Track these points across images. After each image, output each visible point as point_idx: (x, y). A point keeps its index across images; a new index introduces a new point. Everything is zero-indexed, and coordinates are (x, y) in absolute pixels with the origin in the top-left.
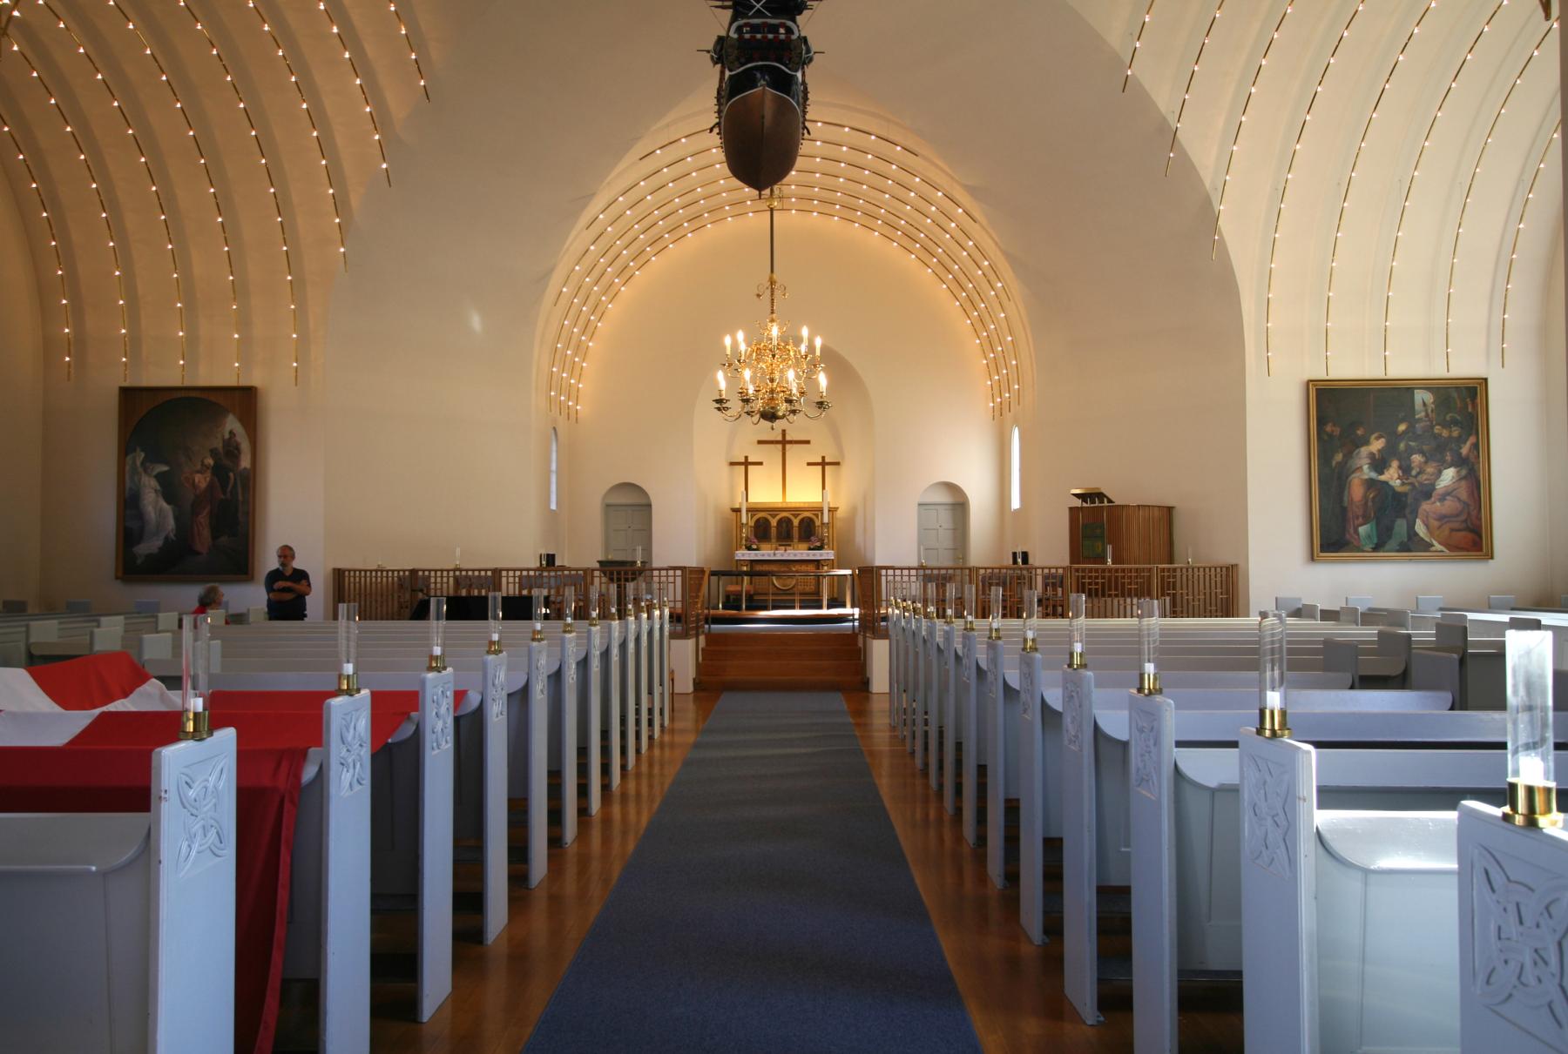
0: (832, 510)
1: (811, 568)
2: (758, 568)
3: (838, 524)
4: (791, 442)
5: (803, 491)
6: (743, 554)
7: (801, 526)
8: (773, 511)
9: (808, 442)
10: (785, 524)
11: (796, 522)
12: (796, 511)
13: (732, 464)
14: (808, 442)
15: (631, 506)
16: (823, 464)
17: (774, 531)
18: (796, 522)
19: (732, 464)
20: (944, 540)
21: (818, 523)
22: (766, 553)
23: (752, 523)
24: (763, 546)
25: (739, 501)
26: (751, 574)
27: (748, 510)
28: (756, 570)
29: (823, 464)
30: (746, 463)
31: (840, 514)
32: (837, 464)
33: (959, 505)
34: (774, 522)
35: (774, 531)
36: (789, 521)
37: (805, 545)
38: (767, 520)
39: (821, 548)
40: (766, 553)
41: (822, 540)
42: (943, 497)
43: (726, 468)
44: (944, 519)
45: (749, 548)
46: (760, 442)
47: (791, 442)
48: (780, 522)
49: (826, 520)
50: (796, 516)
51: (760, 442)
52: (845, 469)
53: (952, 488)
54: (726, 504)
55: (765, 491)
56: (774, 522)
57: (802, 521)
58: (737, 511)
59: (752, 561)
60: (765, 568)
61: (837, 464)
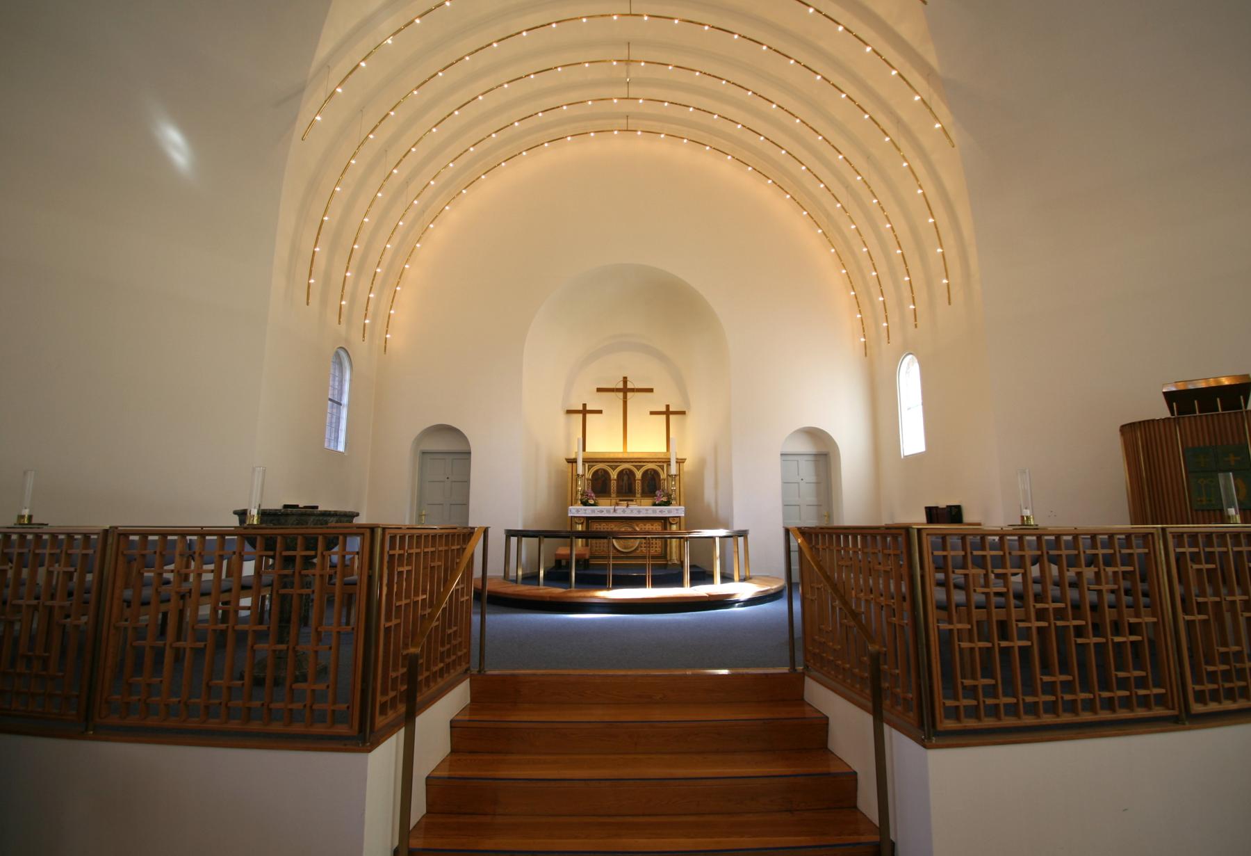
0: (680, 462)
1: (657, 527)
2: (596, 527)
3: (685, 479)
4: (633, 390)
5: (645, 441)
6: (578, 510)
7: (646, 480)
8: (614, 462)
9: (651, 390)
10: (627, 476)
11: (639, 475)
12: (639, 462)
13: (569, 412)
14: (651, 390)
15: (447, 453)
16: (668, 413)
17: (614, 485)
18: (639, 475)
19: (569, 412)
20: (807, 494)
21: (663, 476)
22: (604, 509)
23: (589, 475)
24: (601, 501)
25: (576, 451)
26: (585, 535)
27: (584, 461)
28: (593, 530)
29: (668, 413)
30: (584, 412)
31: (687, 466)
32: (683, 413)
33: (823, 454)
34: (614, 475)
35: (614, 485)
36: (630, 474)
37: (649, 501)
38: (606, 472)
39: (668, 503)
40: (604, 509)
41: (669, 496)
42: (804, 447)
43: (562, 417)
44: (806, 471)
45: (585, 503)
46: (599, 390)
47: (633, 390)
48: (621, 474)
49: (673, 471)
50: (639, 468)
51: (599, 390)
52: (690, 419)
53: (815, 435)
54: (562, 455)
55: (605, 440)
56: (614, 475)
57: (645, 473)
58: (573, 461)
59: (588, 519)
60: (603, 527)
61: (683, 413)
